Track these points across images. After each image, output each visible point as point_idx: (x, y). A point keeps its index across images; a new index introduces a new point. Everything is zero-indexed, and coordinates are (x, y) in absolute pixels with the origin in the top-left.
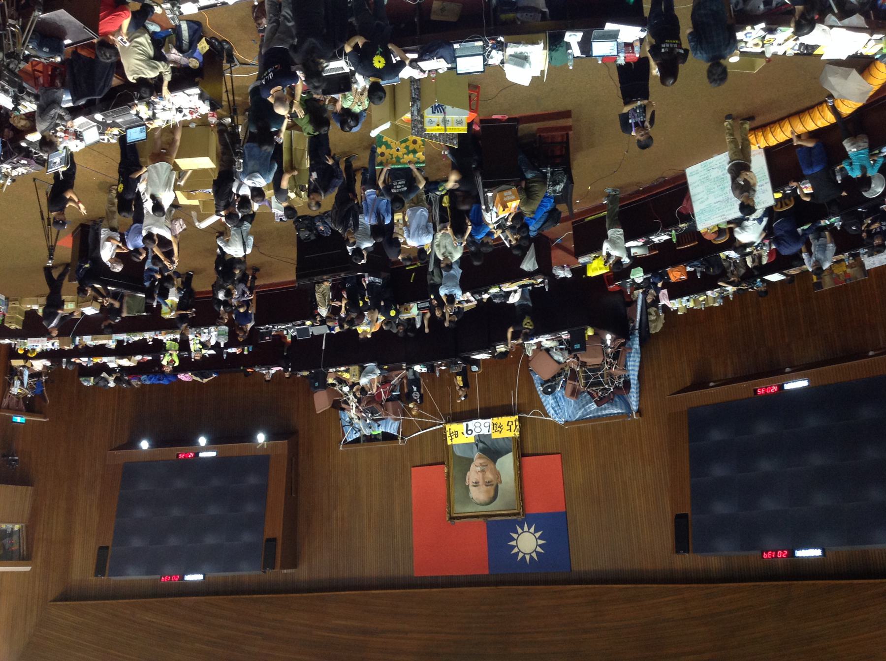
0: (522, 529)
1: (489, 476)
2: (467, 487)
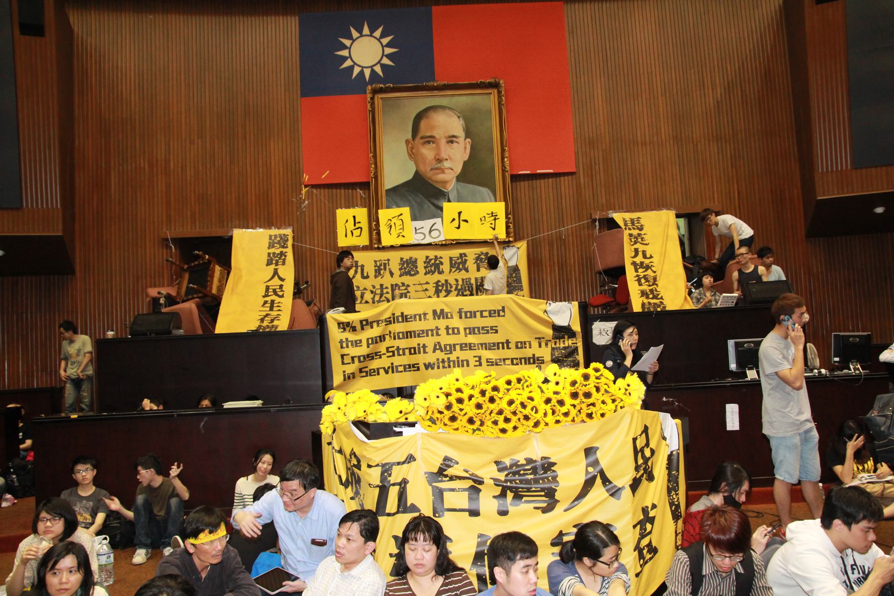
0: (373, 72)
1: (428, 152)
2: (468, 134)
